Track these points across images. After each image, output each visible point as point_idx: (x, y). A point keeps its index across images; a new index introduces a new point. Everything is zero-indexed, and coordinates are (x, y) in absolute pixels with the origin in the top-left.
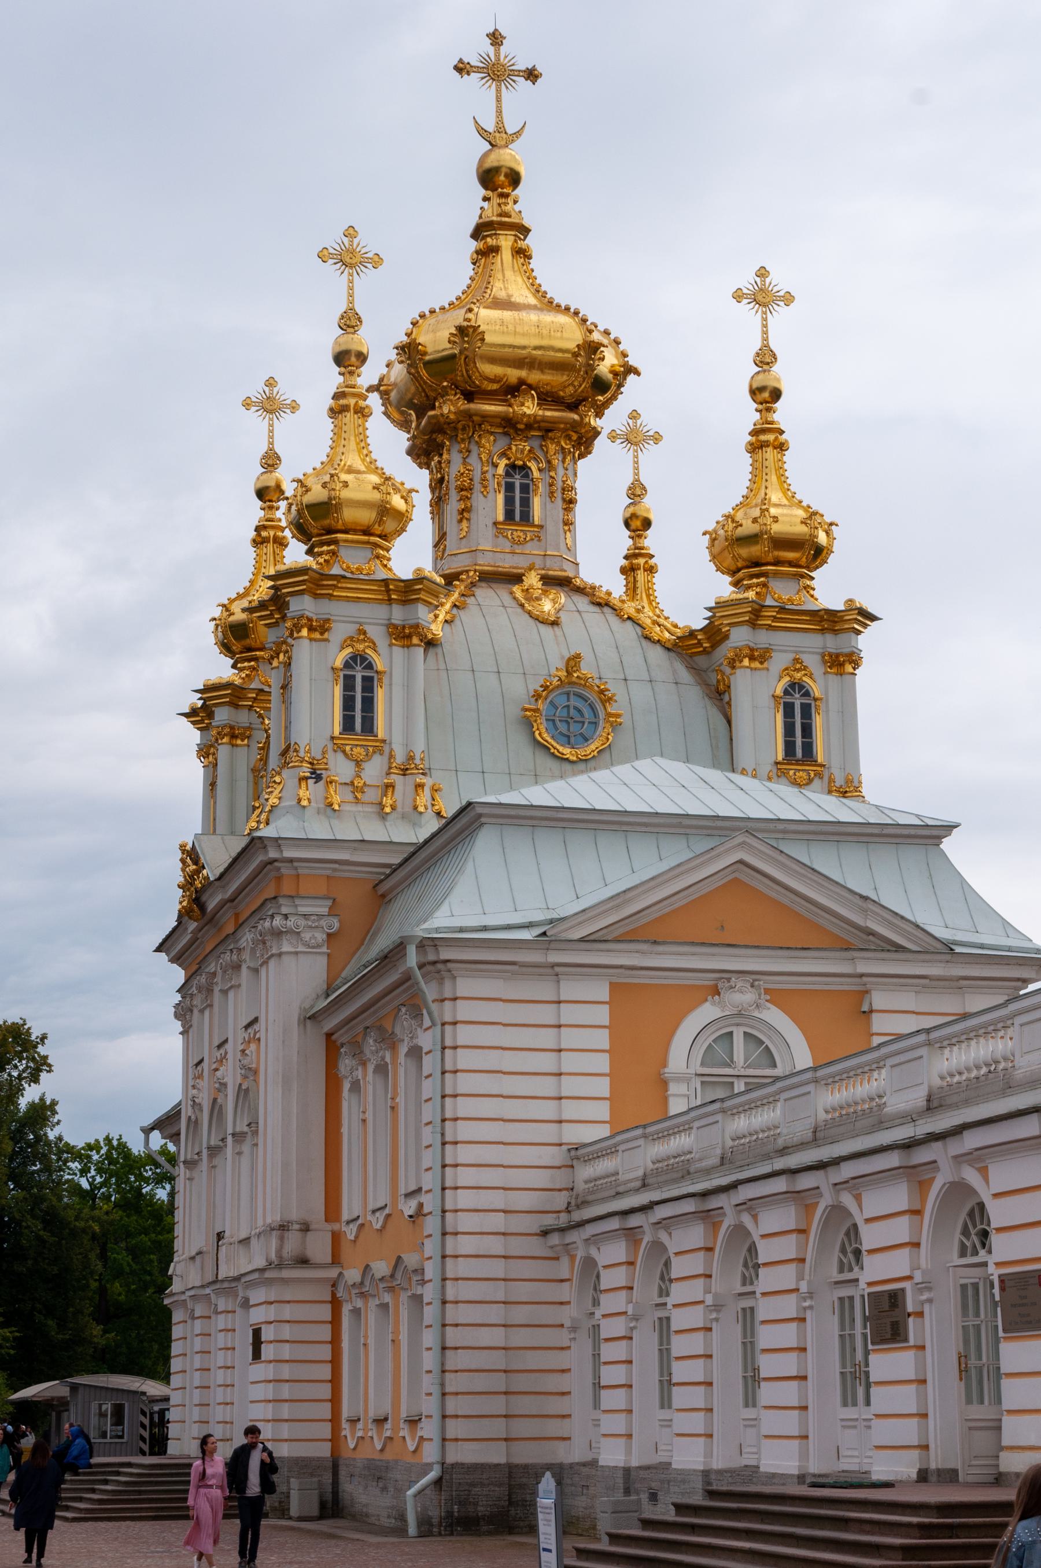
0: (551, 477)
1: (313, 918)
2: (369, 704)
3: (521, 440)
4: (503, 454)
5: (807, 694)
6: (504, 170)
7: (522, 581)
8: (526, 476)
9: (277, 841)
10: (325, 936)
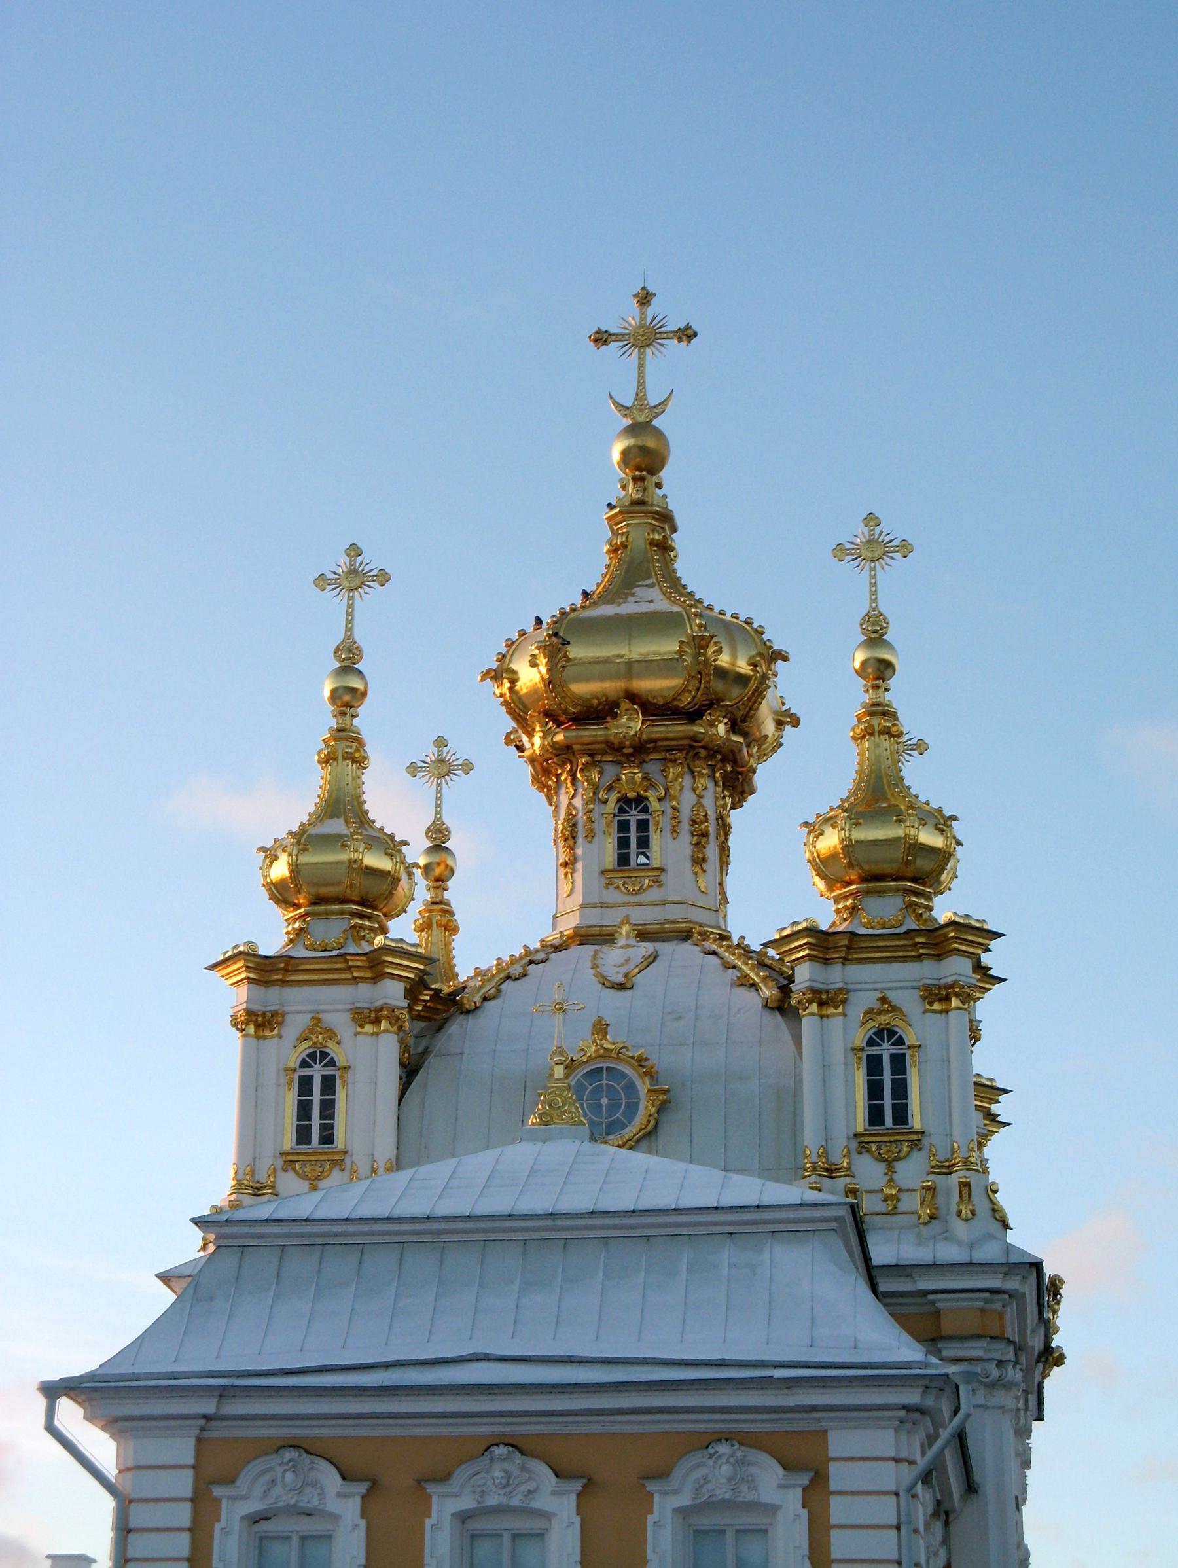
0: (674, 808)
2: (328, 1108)
3: (630, 766)
5: (900, 1041)
8: (645, 810)
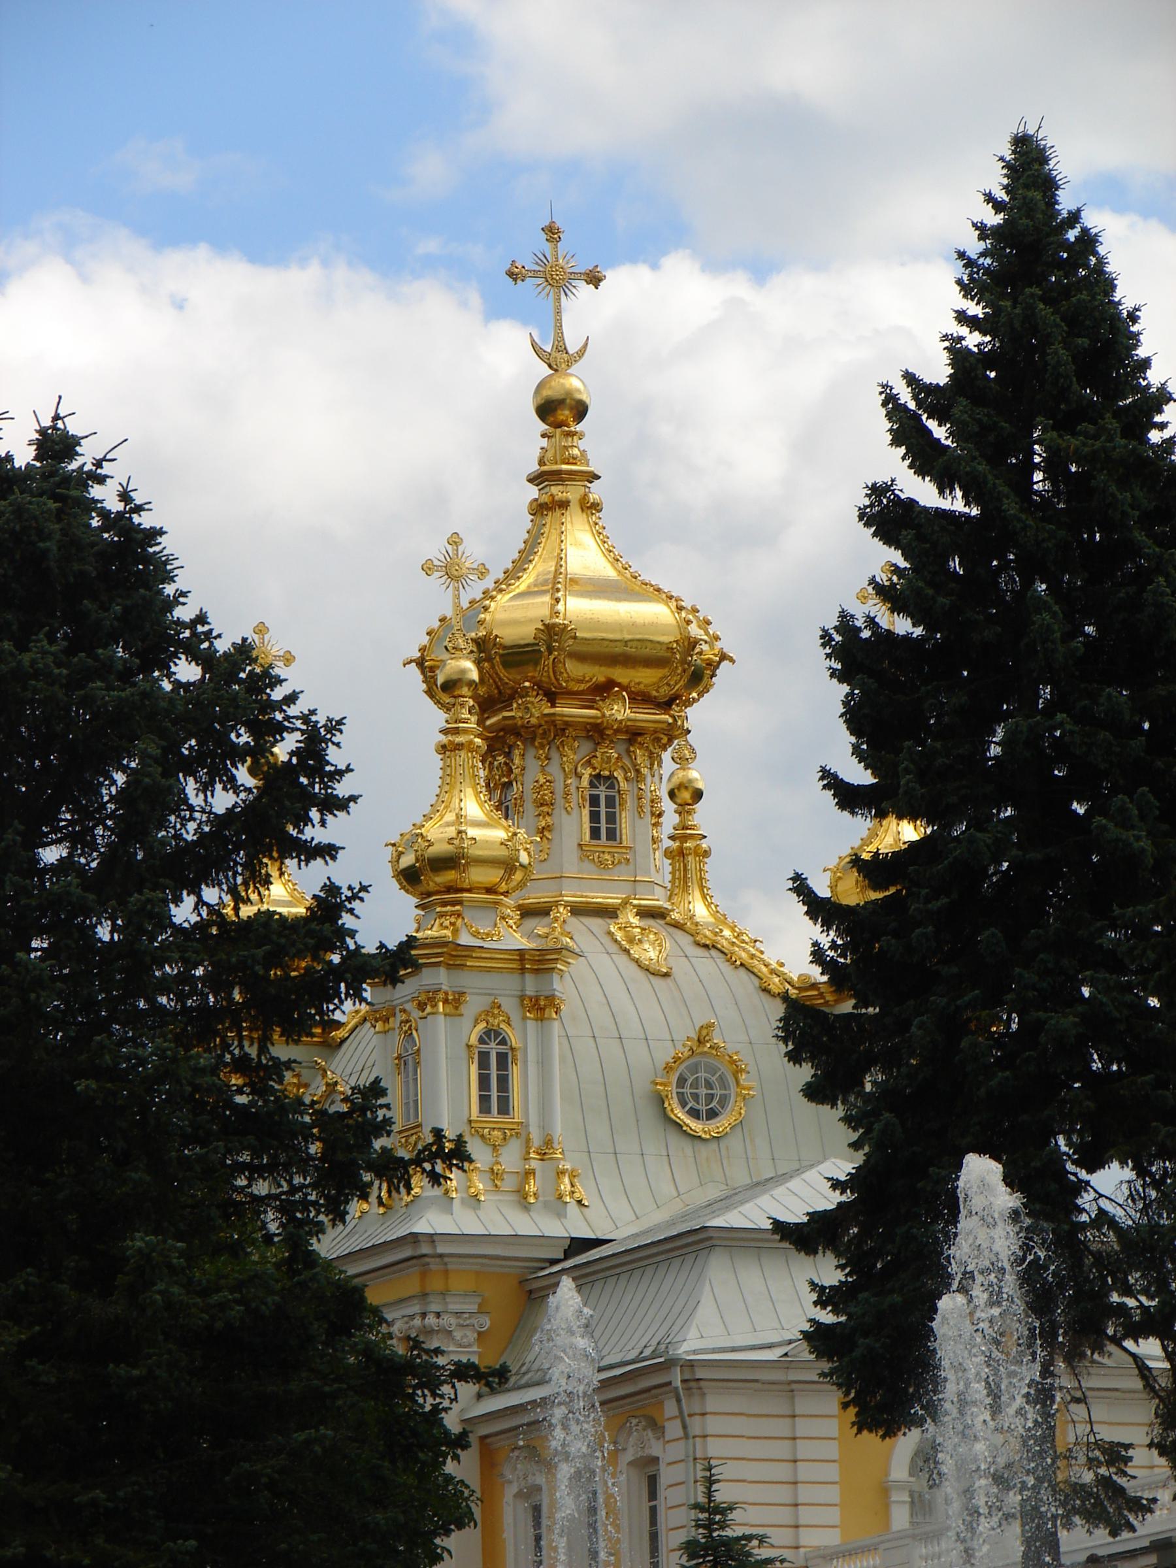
1: (467, 1315)
2: (503, 1082)
4: (589, 763)
6: (568, 401)
7: (617, 917)
8: (611, 787)
9: (432, 1238)
10: (476, 1335)
